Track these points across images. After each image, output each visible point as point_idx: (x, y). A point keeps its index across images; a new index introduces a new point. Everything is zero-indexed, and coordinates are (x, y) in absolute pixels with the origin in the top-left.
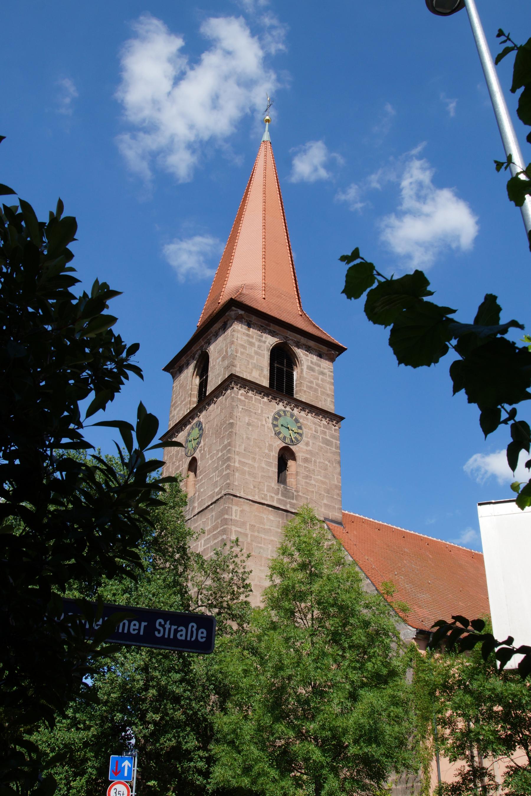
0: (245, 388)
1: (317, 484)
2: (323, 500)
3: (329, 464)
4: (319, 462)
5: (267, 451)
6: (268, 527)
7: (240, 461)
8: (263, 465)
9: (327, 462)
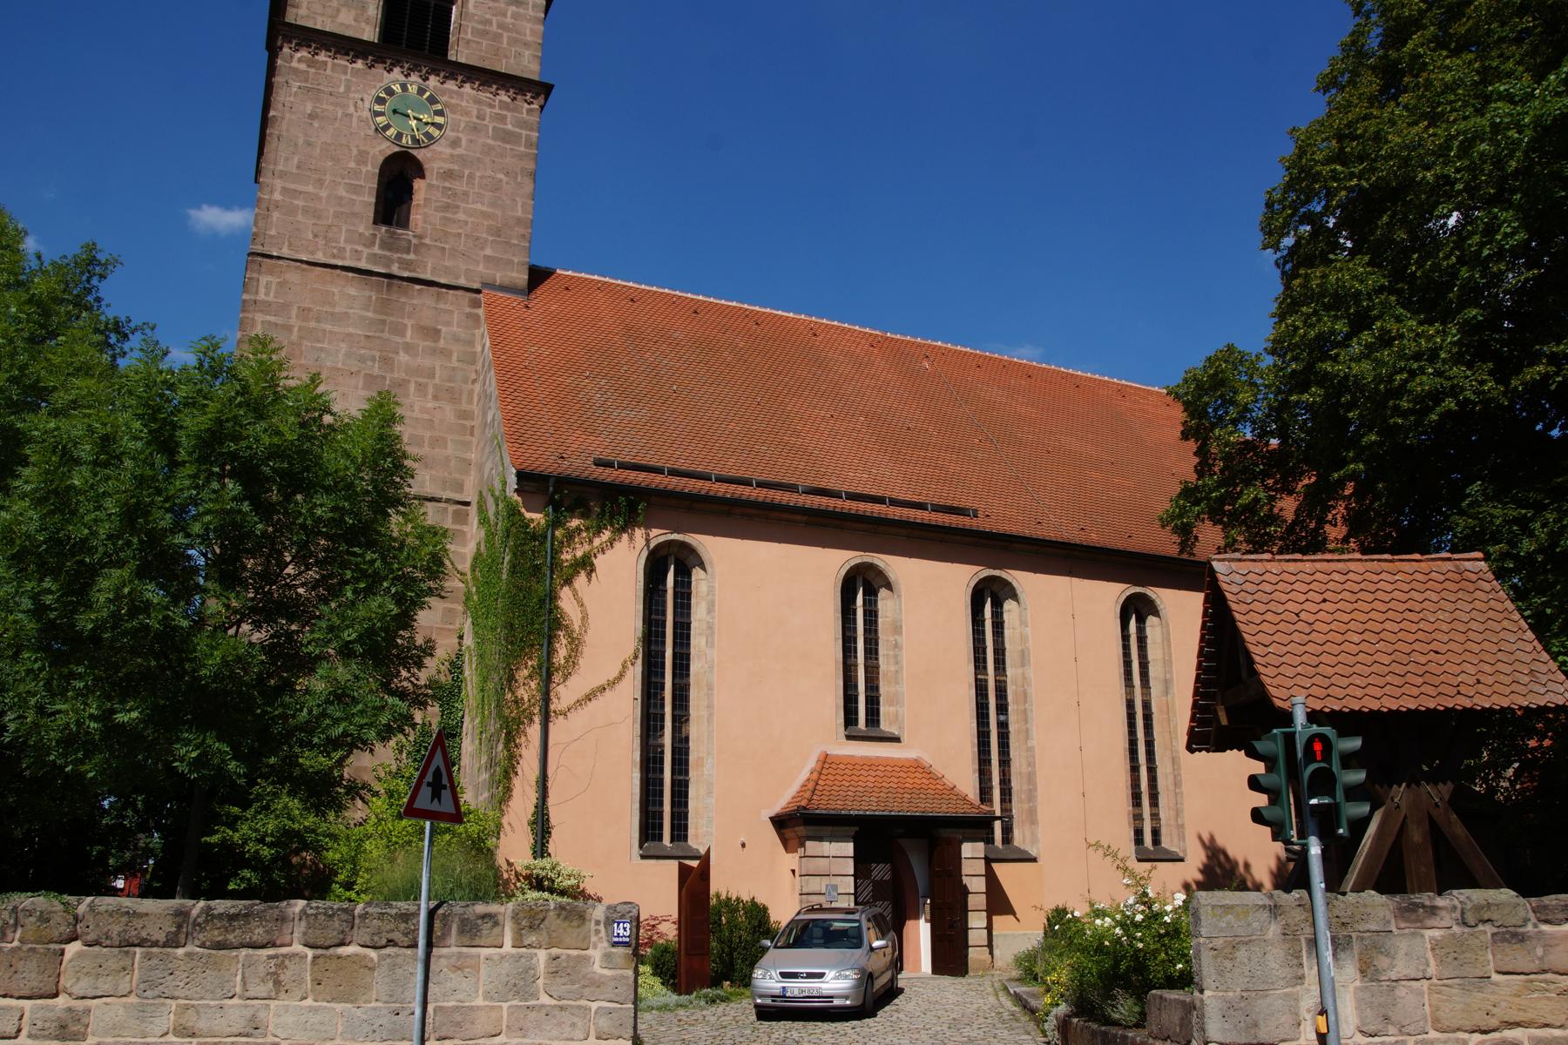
2: (482, 249)
3: (505, 179)
5: (352, 165)
7: (285, 190)
8: (342, 192)
9: (500, 176)
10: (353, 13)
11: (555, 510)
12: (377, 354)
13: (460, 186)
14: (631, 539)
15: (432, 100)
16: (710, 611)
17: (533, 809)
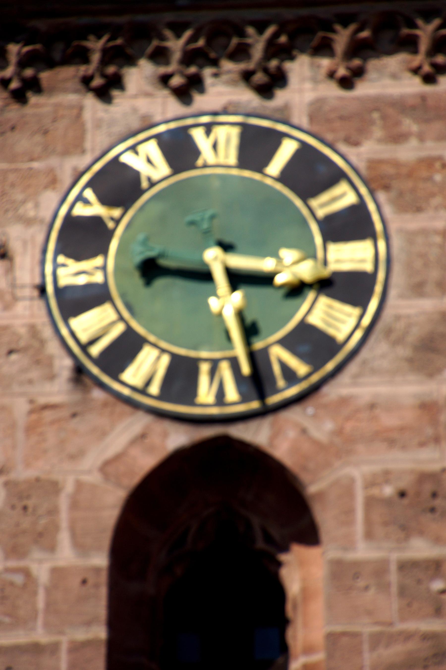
15: (310, 174)
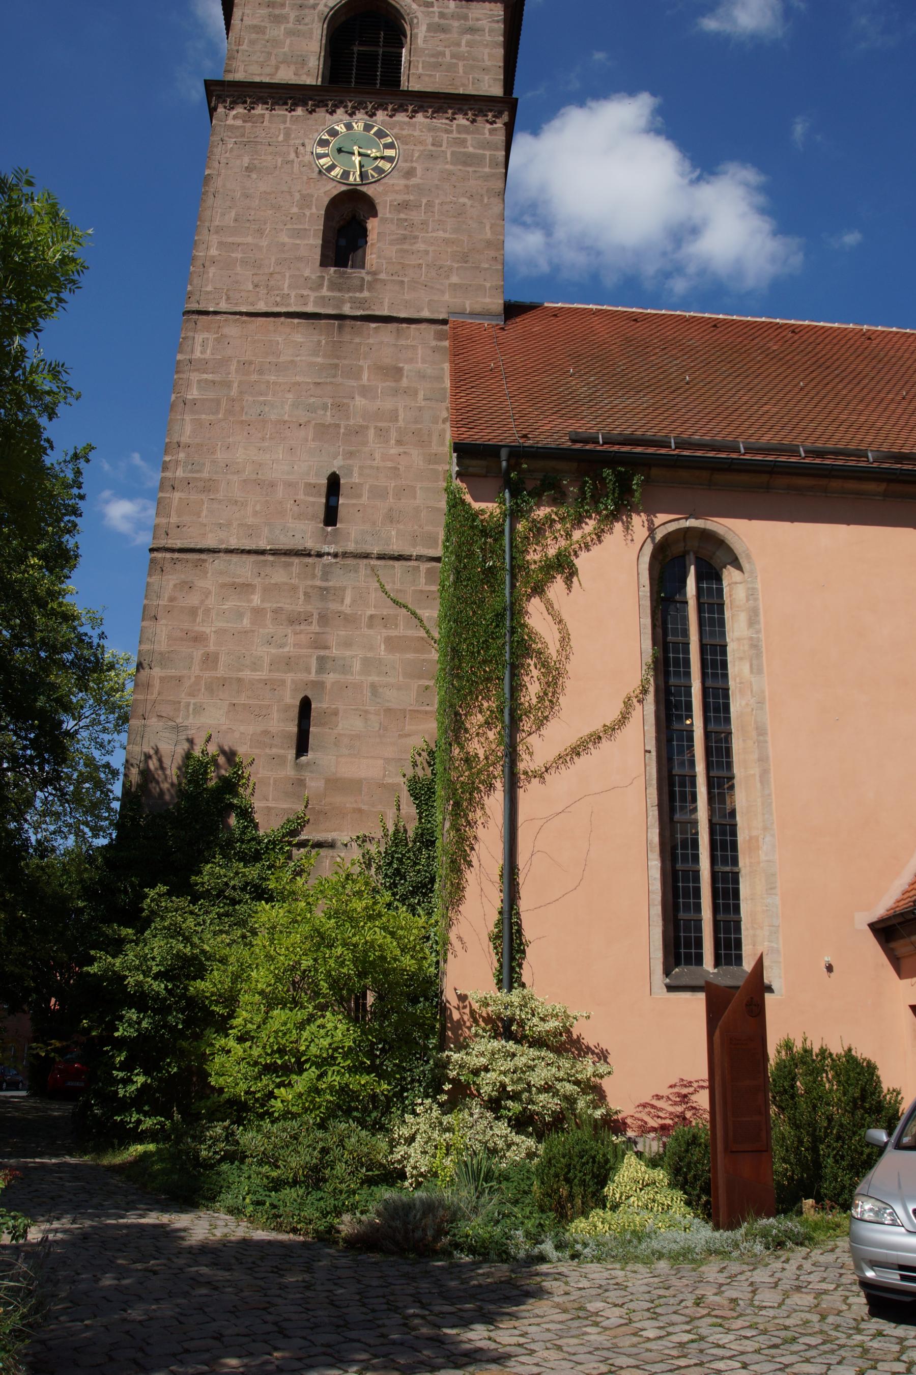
0: (245, 102)
1: (431, 249)
2: (448, 277)
3: (468, 202)
4: (441, 204)
5: (295, 210)
6: (289, 358)
8: (284, 238)
9: (463, 200)
10: (293, 68)
11: (513, 496)
12: (329, 401)
13: (417, 216)
14: (627, 528)
15: (380, 134)
16: (752, 622)
17: (496, 917)
